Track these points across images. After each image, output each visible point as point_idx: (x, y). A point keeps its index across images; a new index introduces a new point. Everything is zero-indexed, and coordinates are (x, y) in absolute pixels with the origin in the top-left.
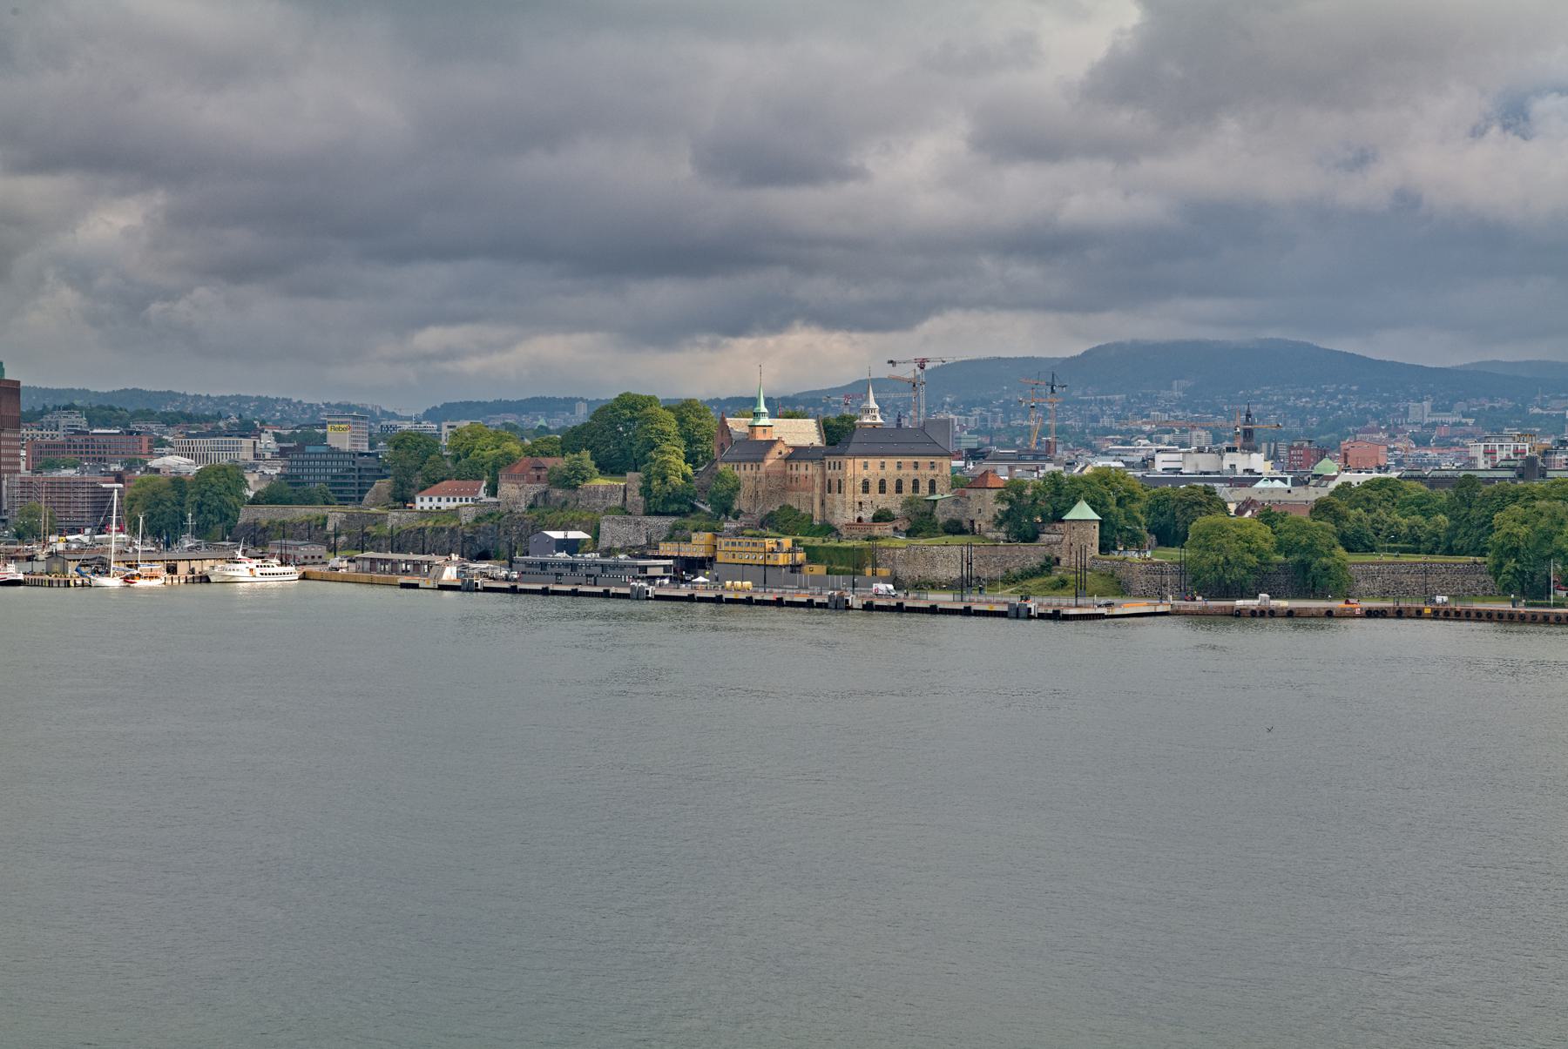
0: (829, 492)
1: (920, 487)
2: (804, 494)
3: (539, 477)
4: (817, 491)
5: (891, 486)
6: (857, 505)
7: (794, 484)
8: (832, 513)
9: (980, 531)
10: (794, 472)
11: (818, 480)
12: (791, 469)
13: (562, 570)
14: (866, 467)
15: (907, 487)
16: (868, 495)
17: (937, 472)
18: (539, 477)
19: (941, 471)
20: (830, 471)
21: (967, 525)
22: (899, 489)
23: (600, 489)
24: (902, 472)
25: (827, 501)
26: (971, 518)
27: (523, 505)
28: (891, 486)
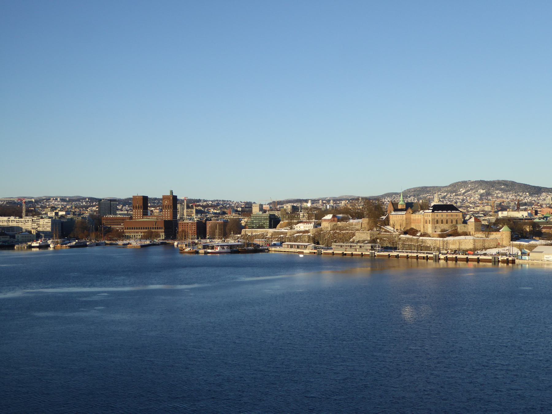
0: (426, 224)
1: (453, 222)
2: (418, 224)
3: (334, 220)
4: (422, 223)
5: (445, 221)
6: (435, 227)
7: (414, 221)
8: (427, 230)
9: (472, 235)
10: (414, 218)
11: (422, 220)
12: (413, 217)
13: (347, 247)
14: (437, 216)
15: (449, 221)
16: (438, 224)
17: (458, 217)
18: (334, 220)
19: (459, 217)
20: (426, 217)
21: (468, 234)
22: (447, 223)
23: (354, 223)
24: (448, 217)
25: (425, 226)
26: (469, 231)
27: (330, 228)
28: (445, 221)
